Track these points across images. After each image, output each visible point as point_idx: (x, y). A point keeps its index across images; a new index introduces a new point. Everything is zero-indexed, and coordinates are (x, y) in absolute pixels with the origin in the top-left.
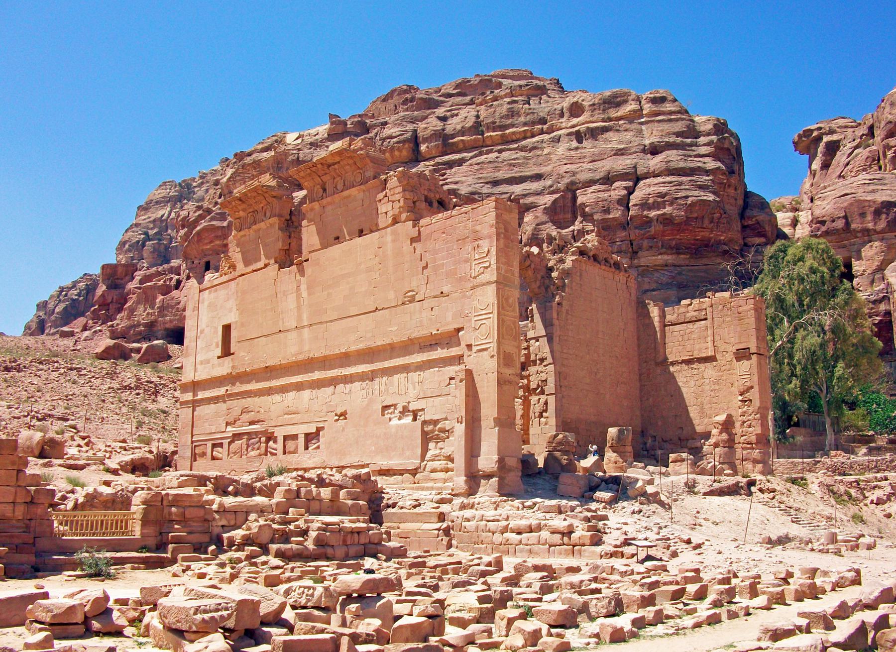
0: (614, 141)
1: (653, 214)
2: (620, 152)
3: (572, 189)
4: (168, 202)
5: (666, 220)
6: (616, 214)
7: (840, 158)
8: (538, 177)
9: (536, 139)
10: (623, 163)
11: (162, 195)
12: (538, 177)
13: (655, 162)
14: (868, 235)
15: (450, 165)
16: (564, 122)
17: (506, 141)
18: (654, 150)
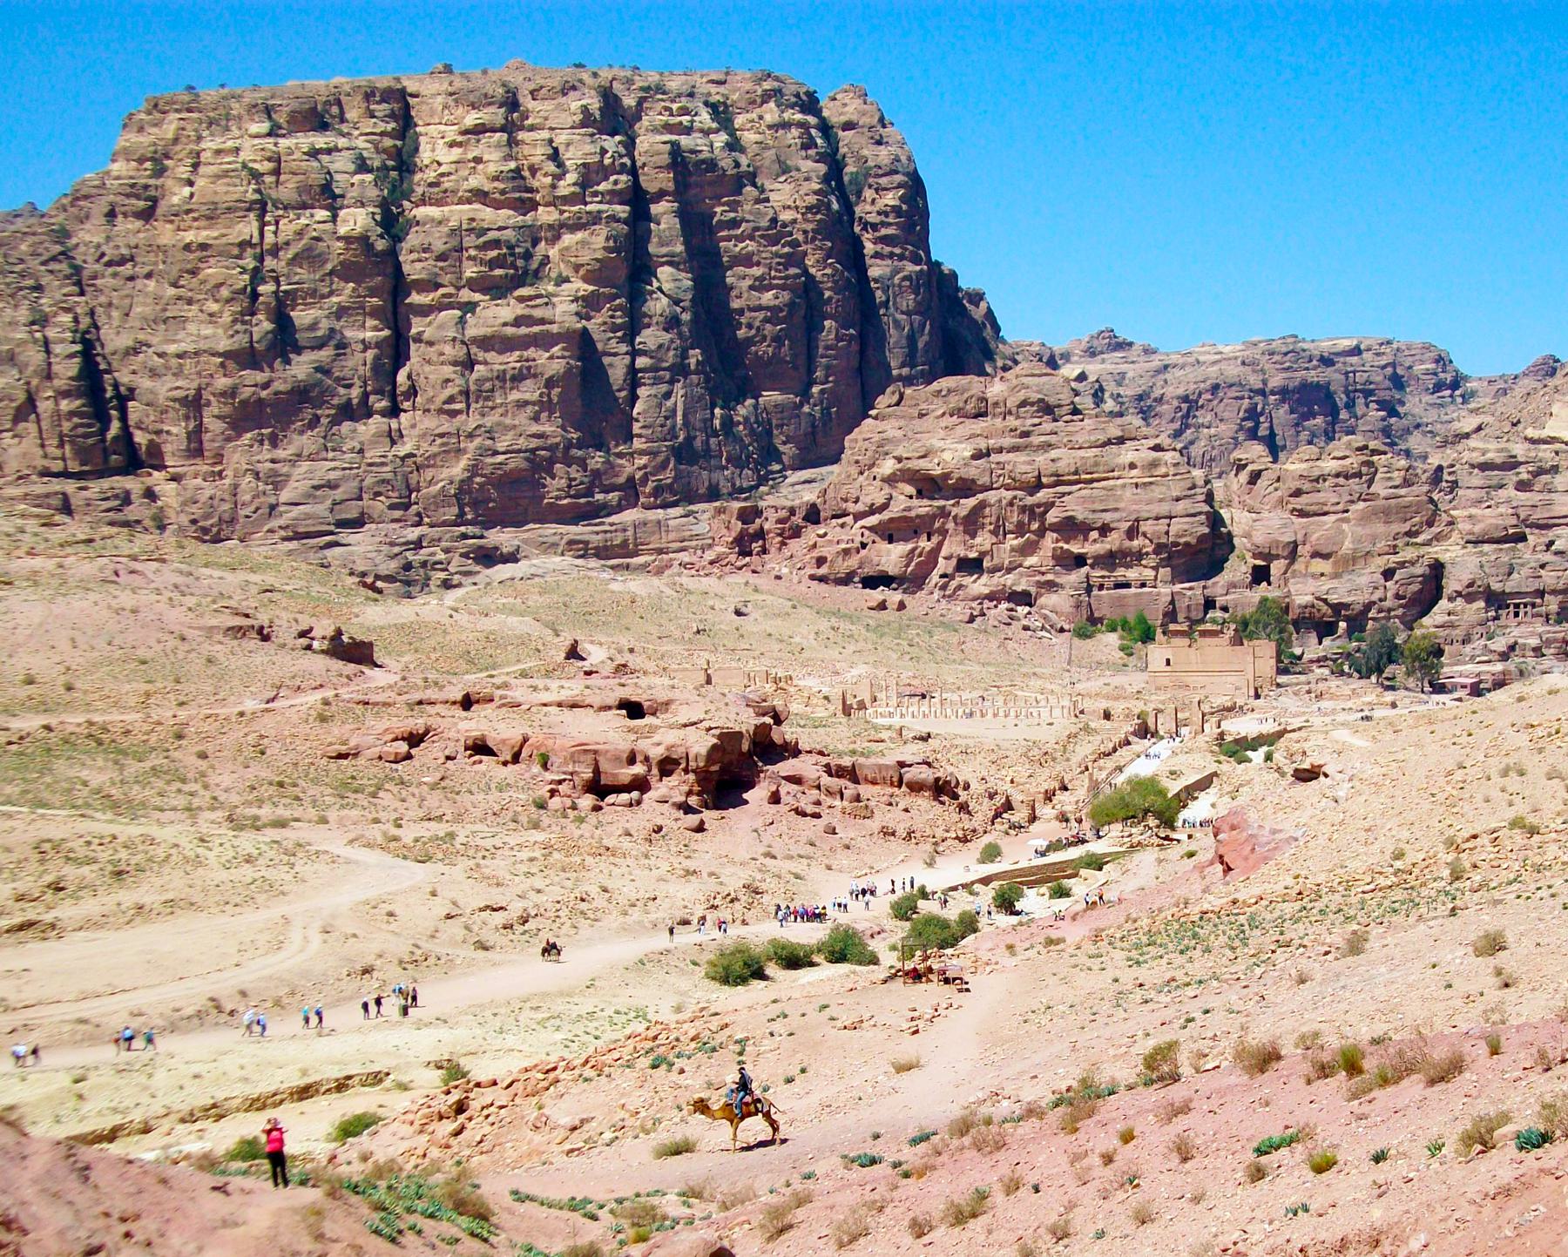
0: (1157, 492)
1: (1182, 540)
2: (1161, 500)
3: (1137, 520)
4: (249, 210)
5: (1187, 544)
6: (1164, 540)
7: (1262, 483)
8: (1116, 510)
9: (1111, 482)
10: (1164, 509)
11: (236, 197)
12: (1116, 510)
13: (1181, 507)
14: (1277, 557)
15: (1064, 494)
16: (1126, 473)
17: (1092, 481)
18: (1178, 500)
